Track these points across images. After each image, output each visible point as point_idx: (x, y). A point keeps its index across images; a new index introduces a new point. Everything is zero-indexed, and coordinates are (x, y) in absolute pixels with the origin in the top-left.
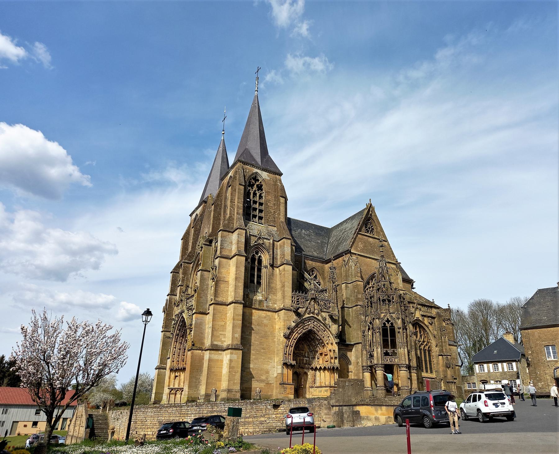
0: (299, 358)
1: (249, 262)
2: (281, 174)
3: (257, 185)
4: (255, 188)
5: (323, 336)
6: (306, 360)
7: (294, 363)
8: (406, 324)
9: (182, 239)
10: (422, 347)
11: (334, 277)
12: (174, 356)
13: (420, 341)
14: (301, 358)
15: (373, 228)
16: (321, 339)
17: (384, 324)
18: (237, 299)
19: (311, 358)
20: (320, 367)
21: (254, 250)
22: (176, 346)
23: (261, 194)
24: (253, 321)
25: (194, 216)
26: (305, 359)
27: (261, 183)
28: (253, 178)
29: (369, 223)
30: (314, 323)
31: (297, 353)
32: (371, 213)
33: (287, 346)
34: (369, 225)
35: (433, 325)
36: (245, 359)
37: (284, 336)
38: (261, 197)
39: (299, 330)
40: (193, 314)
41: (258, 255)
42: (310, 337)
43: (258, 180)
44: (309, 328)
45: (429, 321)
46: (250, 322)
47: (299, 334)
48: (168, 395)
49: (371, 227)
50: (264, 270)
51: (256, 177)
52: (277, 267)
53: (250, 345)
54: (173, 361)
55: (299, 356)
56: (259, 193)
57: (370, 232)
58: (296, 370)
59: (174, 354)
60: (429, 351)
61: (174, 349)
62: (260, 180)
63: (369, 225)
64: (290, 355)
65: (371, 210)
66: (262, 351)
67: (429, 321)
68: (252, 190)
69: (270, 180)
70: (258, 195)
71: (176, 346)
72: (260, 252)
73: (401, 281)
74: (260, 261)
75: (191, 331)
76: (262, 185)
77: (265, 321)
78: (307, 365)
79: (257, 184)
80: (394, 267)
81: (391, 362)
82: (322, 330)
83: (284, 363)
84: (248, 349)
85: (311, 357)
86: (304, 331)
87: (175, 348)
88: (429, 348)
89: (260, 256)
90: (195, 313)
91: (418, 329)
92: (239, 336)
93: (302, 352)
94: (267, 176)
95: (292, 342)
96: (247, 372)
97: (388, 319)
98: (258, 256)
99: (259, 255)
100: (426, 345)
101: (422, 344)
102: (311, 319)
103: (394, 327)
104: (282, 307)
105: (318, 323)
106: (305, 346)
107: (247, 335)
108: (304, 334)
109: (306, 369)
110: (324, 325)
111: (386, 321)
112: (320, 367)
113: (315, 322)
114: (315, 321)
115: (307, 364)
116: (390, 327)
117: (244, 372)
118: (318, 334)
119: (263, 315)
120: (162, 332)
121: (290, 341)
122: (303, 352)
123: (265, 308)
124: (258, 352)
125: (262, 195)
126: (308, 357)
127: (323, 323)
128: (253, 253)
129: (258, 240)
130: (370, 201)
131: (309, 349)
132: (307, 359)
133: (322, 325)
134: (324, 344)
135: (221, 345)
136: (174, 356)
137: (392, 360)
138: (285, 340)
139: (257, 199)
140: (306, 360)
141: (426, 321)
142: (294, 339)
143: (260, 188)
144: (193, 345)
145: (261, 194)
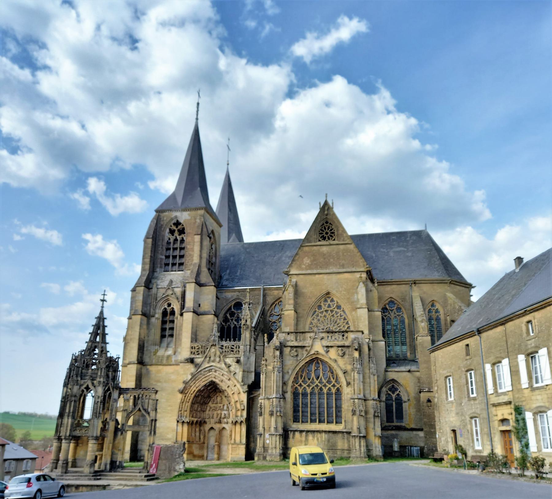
3: (179, 230)
14: (219, 412)
23: (183, 238)
32: (326, 212)
33: (183, 402)
35: (346, 356)
38: (182, 241)
43: (180, 224)
44: (210, 379)
49: (331, 230)
51: (177, 221)
55: (215, 410)
64: (186, 411)
66: (169, 408)
69: (190, 219)
73: (362, 295)
76: (184, 229)
77: (173, 377)
95: (188, 398)
102: (212, 369)
109: (225, 423)
122: (222, 405)
126: (227, 410)
129: (166, 291)
130: (326, 197)
132: (226, 412)
139: (178, 245)
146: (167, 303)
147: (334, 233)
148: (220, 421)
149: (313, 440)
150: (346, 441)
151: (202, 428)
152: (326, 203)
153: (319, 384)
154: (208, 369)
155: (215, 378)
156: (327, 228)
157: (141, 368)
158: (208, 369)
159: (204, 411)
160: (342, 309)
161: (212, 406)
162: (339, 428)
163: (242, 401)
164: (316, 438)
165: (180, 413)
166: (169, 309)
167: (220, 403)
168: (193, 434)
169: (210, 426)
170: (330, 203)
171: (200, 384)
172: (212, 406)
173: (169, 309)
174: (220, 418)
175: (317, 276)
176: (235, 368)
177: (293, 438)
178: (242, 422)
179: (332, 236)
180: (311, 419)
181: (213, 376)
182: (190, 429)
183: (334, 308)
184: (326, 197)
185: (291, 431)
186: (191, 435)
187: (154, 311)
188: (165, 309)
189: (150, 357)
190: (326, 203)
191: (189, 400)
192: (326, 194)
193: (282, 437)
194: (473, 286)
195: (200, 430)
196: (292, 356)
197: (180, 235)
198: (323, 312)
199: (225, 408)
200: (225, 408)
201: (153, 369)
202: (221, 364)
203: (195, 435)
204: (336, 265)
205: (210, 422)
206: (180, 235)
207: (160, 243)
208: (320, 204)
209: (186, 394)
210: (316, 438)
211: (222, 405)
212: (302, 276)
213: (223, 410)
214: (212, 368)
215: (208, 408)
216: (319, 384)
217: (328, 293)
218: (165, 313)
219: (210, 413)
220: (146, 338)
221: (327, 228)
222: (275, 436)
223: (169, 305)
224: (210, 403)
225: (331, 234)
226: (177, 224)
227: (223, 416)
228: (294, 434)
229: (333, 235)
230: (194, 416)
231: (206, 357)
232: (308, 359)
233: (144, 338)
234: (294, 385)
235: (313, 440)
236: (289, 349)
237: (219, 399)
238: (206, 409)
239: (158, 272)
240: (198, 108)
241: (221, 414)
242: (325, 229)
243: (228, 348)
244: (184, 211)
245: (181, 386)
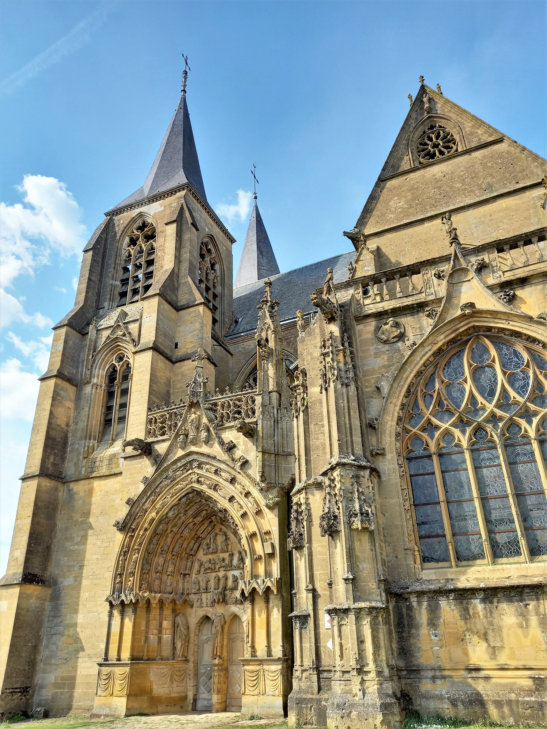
0: (214, 574)
11: (267, 326)
14: (221, 574)
18: (29, 471)
21: (113, 354)
24: (93, 507)
26: (233, 572)
32: (426, 105)
36: (66, 604)
46: (86, 511)
53: (81, 567)
55: (213, 570)
64: (133, 574)
65: (425, 99)
69: (164, 210)
84: (75, 577)
96: (69, 636)
107: (78, 544)
109: (236, 602)
117: (62, 636)
119: (115, 486)
122: (226, 555)
124: (95, 582)
129: (113, 332)
133: (223, 466)
147: (453, 140)
148: (225, 596)
149: (524, 626)
151: (179, 620)
152: (423, 89)
153: (499, 412)
154: (183, 462)
155: (198, 482)
156: (433, 136)
157: (56, 489)
158: (183, 462)
159: (185, 575)
161: (205, 559)
163: (268, 533)
164: (534, 620)
165: (118, 580)
167: (223, 551)
168: (153, 638)
169: (201, 613)
170: (431, 85)
174: (225, 589)
175: (427, 225)
176: (247, 451)
177: (433, 623)
178: (268, 590)
180: (494, 545)
181: (195, 477)
182: (144, 623)
185: (420, 594)
186: (147, 639)
187: (88, 372)
189: (76, 464)
191: (140, 544)
193: (387, 622)
195: (175, 626)
196: (385, 342)
199: (235, 561)
200: (235, 561)
201: (79, 488)
202: (211, 446)
203: (160, 639)
204: (472, 191)
205: (202, 602)
207: (111, 261)
208: (410, 97)
209: (134, 531)
211: (226, 555)
212: (389, 236)
213: (230, 567)
214: (191, 458)
215: (196, 566)
216: (499, 412)
219: (201, 577)
220: (72, 427)
221: (433, 136)
222: (352, 617)
223: (121, 358)
224: (201, 553)
225: (446, 144)
228: (434, 610)
229: (451, 145)
230: (156, 588)
231: (177, 435)
232: (441, 340)
233: (67, 425)
234: (407, 431)
235: (524, 626)
236: (372, 324)
237: (220, 539)
238: (191, 569)
239: (106, 308)
240: (185, 78)
241: (226, 578)
243: (229, 406)
244: (153, 201)
245: (122, 512)
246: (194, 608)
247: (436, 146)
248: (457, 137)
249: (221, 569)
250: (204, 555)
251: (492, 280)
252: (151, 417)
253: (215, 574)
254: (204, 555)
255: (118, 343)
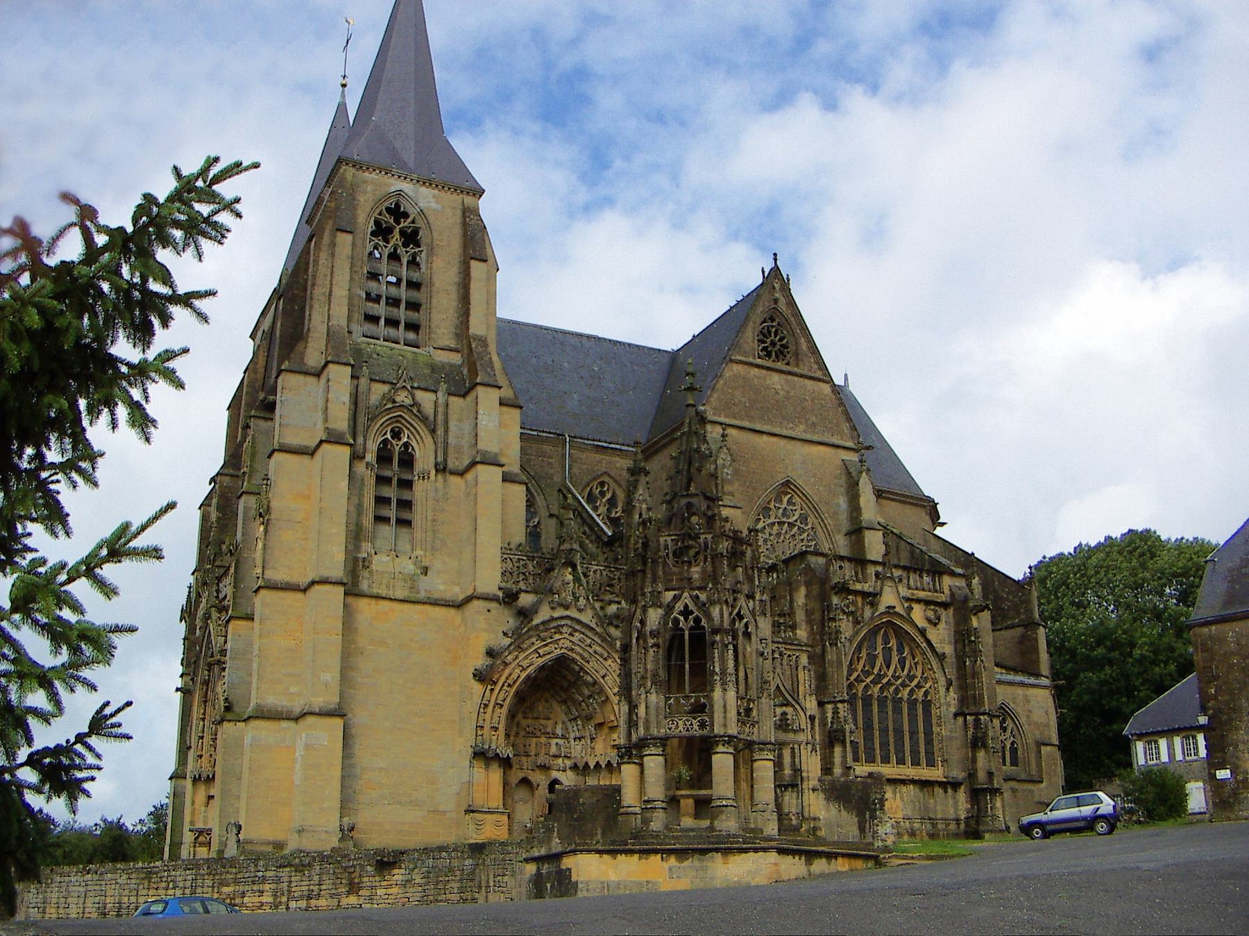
0: (534, 740)
1: (367, 464)
2: (479, 192)
3: (403, 233)
4: (396, 238)
5: (603, 672)
6: (557, 743)
7: (508, 752)
8: (745, 620)
9: (228, 409)
10: (905, 693)
12: (201, 741)
13: (899, 677)
15: (785, 341)
16: (595, 683)
17: (676, 621)
19: (575, 739)
20: (598, 763)
21: (389, 425)
22: (204, 714)
23: (414, 256)
25: (259, 334)
26: (555, 741)
27: (413, 222)
28: (388, 209)
29: (773, 326)
30: (571, 634)
31: (528, 726)
33: (486, 706)
34: (773, 335)
37: (475, 675)
38: (413, 263)
39: (526, 658)
40: (228, 622)
41: (400, 439)
42: (564, 677)
43: (406, 215)
44: (558, 652)
45: (931, 614)
47: (524, 669)
48: (192, 849)
50: (419, 486)
51: (398, 205)
52: (462, 474)
54: (201, 756)
56: (407, 252)
57: (777, 357)
58: (523, 775)
59: (202, 738)
60: (927, 705)
61: (202, 723)
62: (413, 213)
63: (773, 335)
64: (496, 729)
67: (931, 614)
68: (386, 247)
70: (405, 261)
71: (204, 714)
72: (406, 431)
74: (407, 461)
75: (224, 669)
76: (416, 232)
78: (560, 760)
79: (401, 225)
80: (853, 459)
81: (688, 730)
82: (601, 656)
83: (475, 753)
85: (572, 735)
86: (540, 661)
87: (203, 719)
88: (926, 693)
89: (406, 445)
90: (231, 618)
91: (893, 643)
92: (332, 677)
93: (542, 722)
94: (433, 200)
97: (686, 606)
98: (401, 443)
99: (406, 440)
100: (919, 686)
101: (904, 685)
103: (703, 628)
104: (469, 593)
105: (584, 634)
106: (555, 704)
108: (542, 668)
110: (604, 640)
111: (681, 613)
112: (598, 763)
113: (577, 634)
114: (576, 631)
115: (559, 756)
116: (691, 629)
118: (587, 667)
120: (181, 676)
121: (496, 691)
122: (550, 723)
123: (422, 595)
125: (418, 258)
126: (563, 737)
127: (600, 636)
128: (385, 434)
130: (775, 260)
131: (567, 713)
132: (560, 741)
134: (608, 697)
135: (289, 704)
136: (201, 741)
137: (691, 724)
138: (478, 688)
140: (557, 743)
141: (918, 615)
142: (509, 685)
143: (411, 238)
144: (228, 709)
145: (414, 256)
146: (390, 428)
150: (951, 801)
160: (810, 526)
161: (524, 723)
162: (937, 774)
166: (397, 446)
169: (521, 775)
171: (529, 661)
172: (524, 723)
173: (397, 446)
175: (765, 438)
179: (782, 353)
183: (796, 521)
184: (775, 260)
188: (385, 442)
190: (776, 271)
192: (775, 255)
194: (941, 520)
197: (405, 245)
198: (773, 524)
206: (405, 245)
209: (495, 683)
210: (898, 795)
214: (563, 622)
217: (787, 483)
218: (384, 456)
226: (397, 213)
227: (553, 750)
242: (770, 333)
245: (481, 661)
246: (514, 769)
247: (773, 344)
248: (792, 348)
249: (543, 736)
250: (524, 718)
251: (904, 591)
252: (505, 556)
253: (536, 739)
254: (524, 718)
255: (404, 415)
